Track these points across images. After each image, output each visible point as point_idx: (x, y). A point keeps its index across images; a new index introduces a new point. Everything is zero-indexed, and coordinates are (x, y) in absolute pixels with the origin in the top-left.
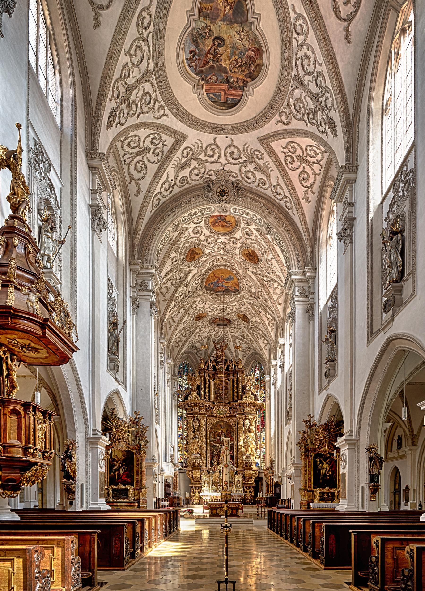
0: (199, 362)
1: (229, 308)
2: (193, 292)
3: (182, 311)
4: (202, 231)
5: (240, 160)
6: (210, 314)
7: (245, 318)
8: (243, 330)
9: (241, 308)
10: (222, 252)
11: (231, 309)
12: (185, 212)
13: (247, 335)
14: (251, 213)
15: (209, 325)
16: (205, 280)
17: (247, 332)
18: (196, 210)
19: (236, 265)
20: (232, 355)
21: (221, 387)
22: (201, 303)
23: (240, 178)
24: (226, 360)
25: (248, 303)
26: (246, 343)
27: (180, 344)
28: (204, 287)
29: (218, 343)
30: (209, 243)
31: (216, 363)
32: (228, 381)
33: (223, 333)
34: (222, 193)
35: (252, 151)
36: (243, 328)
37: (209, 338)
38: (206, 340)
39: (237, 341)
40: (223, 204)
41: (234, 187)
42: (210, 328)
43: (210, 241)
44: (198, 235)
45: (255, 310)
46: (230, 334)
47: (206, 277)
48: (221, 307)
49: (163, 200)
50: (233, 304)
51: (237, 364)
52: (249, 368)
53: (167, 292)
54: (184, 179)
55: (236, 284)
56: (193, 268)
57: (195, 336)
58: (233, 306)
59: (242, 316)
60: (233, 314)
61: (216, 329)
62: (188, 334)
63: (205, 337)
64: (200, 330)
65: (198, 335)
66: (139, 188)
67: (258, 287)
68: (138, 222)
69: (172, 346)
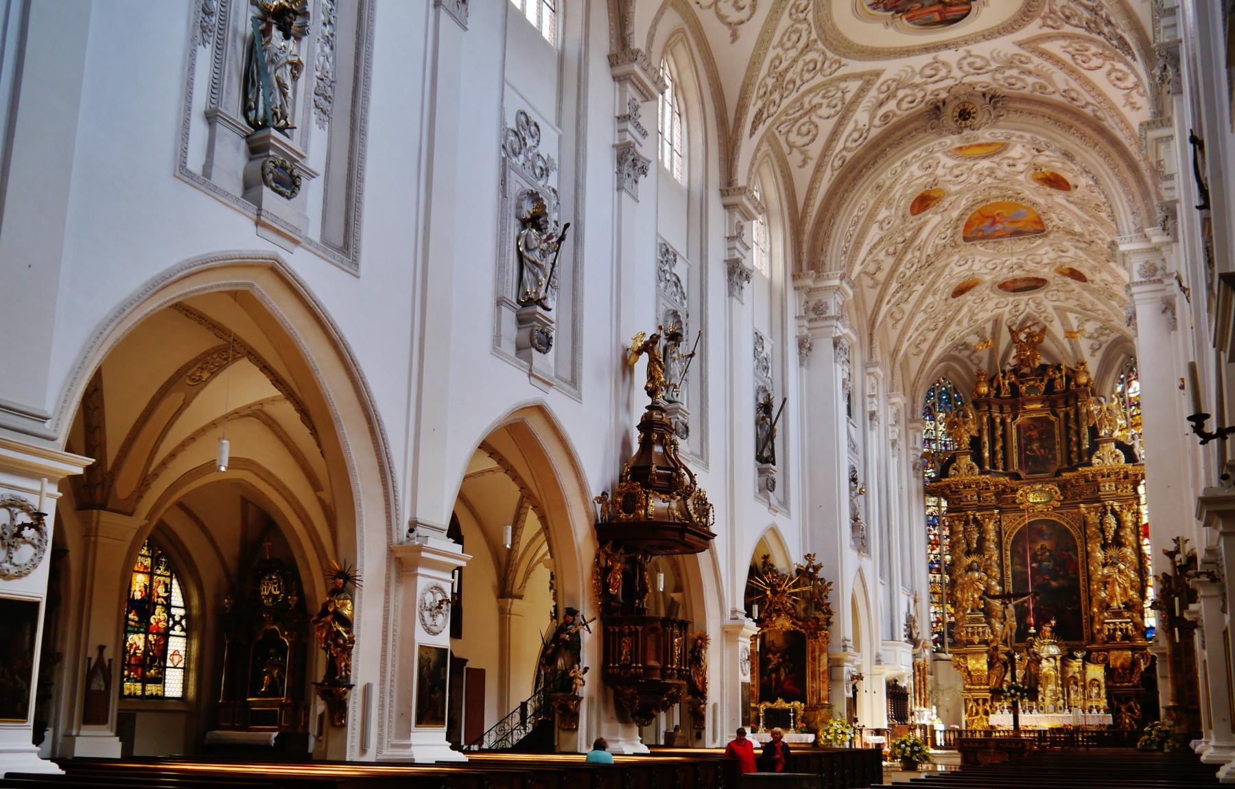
1: (1031, 260)
2: (937, 255)
3: (919, 288)
6: (988, 278)
7: (1076, 275)
8: (1079, 293)
9: (1061, 257)
10: (989, 180)
11: (1038, 259)
12: (894, 162)
13: (1092, 304)
15: (992, 295)
16: (961, 229)
17: (1091, 298)
18: (917, 152)
20: (1063, 350)
21: (1034, 434)
22: (962, 263)
23: (994, 85)
24: (1044, 367)
25: (1076, 247)
26: (1095, 319)
27: (925, 347)
28: (960, 240)
29: (1021, 330)
30: (957, 176)
32: (1052, 418)
33: (1032, 305)
34: (965, 114)
35: (1009, 56)
37: (997, 322)
38: (989, 327)
39: (1071, 317)
40: (967, 132)
42: (996, 301)
43: (959, 173)
44: (929, 171)
45: (1095, 260)
46: (1048, 305)
47: (962, 225)
48: (1014, 260)
49: (849, 156)
50: (1042, 251)
51: (1072, 375)
53: (879, 269)
54: (886, 116)
55: (1035, 222)
56: (930, 216)
57: (959, 323)
58: (1041, 255)
59: (1067, 272)
60: (1046, 270)
61: (1011, 299)
62: (940, 325)
63: (988, 320)
64: (970, 310)
65: (965, 322)
69: (906, 355)
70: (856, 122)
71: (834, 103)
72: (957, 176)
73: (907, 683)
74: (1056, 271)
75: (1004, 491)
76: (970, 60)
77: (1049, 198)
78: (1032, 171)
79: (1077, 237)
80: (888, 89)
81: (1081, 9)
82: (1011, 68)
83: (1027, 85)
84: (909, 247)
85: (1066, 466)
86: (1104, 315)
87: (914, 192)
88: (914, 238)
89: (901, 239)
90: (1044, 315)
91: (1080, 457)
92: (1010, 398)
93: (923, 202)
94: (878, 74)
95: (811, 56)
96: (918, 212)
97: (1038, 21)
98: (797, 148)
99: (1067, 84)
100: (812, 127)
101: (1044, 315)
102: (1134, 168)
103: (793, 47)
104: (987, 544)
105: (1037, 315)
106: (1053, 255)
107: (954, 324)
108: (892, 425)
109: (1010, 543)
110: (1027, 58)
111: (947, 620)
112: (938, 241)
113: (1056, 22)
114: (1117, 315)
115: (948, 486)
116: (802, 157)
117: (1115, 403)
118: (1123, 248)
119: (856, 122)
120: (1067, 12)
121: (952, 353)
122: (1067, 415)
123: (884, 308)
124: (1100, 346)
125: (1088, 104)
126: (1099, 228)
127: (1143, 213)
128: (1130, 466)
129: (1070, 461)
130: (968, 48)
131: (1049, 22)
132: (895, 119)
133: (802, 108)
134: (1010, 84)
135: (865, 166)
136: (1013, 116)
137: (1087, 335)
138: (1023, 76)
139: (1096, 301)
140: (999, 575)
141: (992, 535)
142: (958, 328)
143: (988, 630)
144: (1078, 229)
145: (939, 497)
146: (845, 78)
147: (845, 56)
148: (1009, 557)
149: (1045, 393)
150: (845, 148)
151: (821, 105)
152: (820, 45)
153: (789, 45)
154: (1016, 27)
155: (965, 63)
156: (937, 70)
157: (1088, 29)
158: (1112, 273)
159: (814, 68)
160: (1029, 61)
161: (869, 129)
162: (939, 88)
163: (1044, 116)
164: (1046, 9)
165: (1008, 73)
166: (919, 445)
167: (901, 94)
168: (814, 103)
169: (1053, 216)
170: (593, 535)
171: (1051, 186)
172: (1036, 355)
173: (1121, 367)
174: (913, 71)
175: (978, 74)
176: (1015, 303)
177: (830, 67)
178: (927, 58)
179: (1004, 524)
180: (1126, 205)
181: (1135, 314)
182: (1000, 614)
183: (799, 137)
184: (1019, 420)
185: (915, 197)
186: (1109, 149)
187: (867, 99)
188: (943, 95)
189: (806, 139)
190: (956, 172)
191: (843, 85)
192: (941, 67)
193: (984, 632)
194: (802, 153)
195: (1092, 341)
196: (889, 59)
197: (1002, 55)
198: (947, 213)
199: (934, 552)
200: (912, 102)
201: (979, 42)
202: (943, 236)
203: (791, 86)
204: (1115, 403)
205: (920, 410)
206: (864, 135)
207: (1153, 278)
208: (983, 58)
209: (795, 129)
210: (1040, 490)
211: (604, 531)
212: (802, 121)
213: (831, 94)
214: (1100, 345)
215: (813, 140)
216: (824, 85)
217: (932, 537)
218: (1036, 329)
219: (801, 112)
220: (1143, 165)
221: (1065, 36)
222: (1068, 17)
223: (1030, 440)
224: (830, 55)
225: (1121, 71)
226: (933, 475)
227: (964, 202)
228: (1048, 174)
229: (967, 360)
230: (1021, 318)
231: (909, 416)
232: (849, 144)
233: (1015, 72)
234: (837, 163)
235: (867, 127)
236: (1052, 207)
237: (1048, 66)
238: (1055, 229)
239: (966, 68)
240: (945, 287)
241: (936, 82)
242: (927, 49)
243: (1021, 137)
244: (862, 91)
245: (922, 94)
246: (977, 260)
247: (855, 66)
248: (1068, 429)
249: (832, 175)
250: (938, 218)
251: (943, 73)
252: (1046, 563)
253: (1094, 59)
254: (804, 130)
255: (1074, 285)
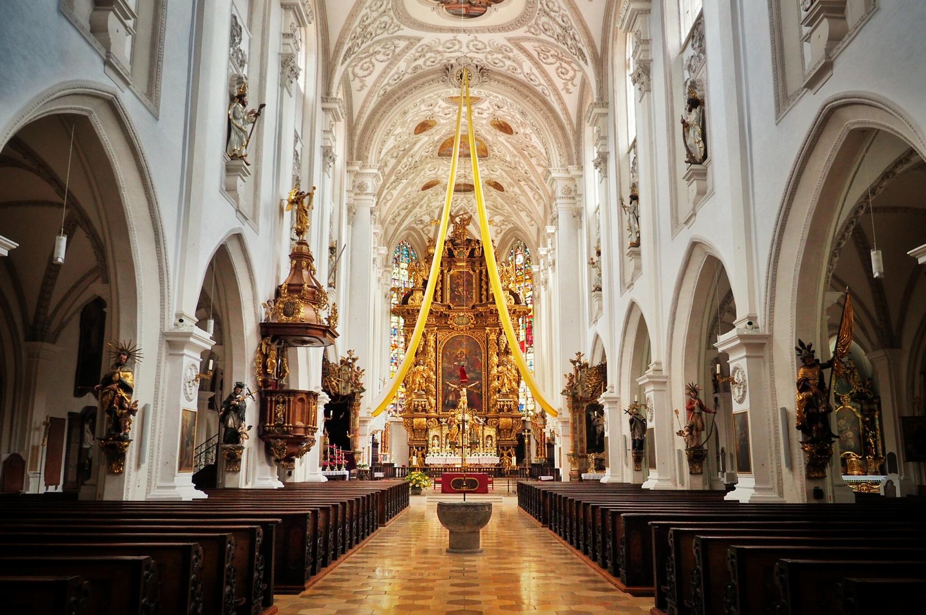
0: (428, 244)
2: (421, 162)
4: (437, 104)
5: (485, 50)
7: (498, 187)
12: (416, 99)
13: (502, 205)
14: (500, 97)
16: (439, 147)
17: (502, 201)
18: (431, 95)
19: (483, 131)
21: (461, 281)
22: (432, 169)
23: (485, 62)
24: (469, 241)
25: (502, 170)
26: (501, 215)
27: (398, 219)
30: (446, 114)
31: (453, 245)
32: (471, 272)
35: (499, 45)
36: (495, 195)
38: (437, 211)
41: (478, 71)
43: (448, 112)
44: (431, 108)
45: (512, 179)
47: (440, 144)
49: (389, 89)
52: (506, 250)
54: (416, 68)
55: (483, 151)
57: (421, 207)
62: (410, 206)
65: (425, 206)
66: (364, 84)
67: (515, 156)
68: (359, 117)
70: (398, 68)
71: (388, 52)
72: (446, 114)
73: (378, 437)
74: (486, 182)
75: (441, 316)
76: (475, 43)
77: (495, 137)
78: (492, 119)
79: (507, 164)
80: (422, 51)
81: (557, 27)
82: (499, 53)
83: (505, 65)
84: (406, 154)
85: (478, 303)
86: (507, 213)
87: (419, 119)
88: (410, 149)
89: (403, 149)
90: (471, 208)
91: (487, 299)
92: (448, 258)
93: (423, 127)
94: (419, 40)
95: (385, 18)
96: (419, 133)
97: (525, 28)
98: (358, 77)
99: (531, 70)
100: (371, 65)
101: (471, 208)
102: (562, 128)
103: (377, 10)
104: (429, 348)
105: (466, 208)
106: (486, 172)
107: (418, 206)
108: (379, 268)
109: (442, 349)
110: (510, 49)
111: (400, 396)
112: (423, 153)
113: (536, 31)
114: (515, 214)
115: (408, 310)
116: (360, 84)
117: (511, 267)
118: (554, 175)
119: (398, 68)
120: (546, 27)
121: (413, 225)
122: (481, 272)
123: (385, 191)
124: (501, 231)
125: (540, 84)
126: (522, 160)
127: (565, 155)
128: (517, 307)
129: (481, 301)
130: (477, 35)
131: (532, 30)
132: (419, 71)
133: (368, 52)
134: (494, 63)
135: (398, 98)
136: (494, 84)
137: (494, 224)
138: (504, 60)
139: (505, 204)
140: (434, 369)
141: (432, 343)
142: (420, 210)
143: (427, 404)
144: (508, 159)
145: (399, 316)
146: (399, 38)
147: (404, 25)
148: (441, 358)
149: (468, 257)
150: (388, 84)
151: (380, 52)
152: (392, 13)
153: (374, 8)
154: (511, 28)
155: (471, 44)
156: (454, 45)
157: (558, 39)
158: (520, 188)
159: (385, 27)
160: (511, 51)
161: (404, 74)
162: (450, 57)
163: (512, 87)
164: (533, 22)
165: (495, 56)
166: (389, 282)
167: (428, 55)
168: (375, 50)
169: (495, 149)
170: (257, 331)
171: (501, 130)
172: (464, 232)
173: (512, 245)
174: (439, 43)
175: (477, 53)
176: (455, 199)
177: (393, 29)
178: (450, 36)
179: (438, 336)
180: (556, 149)
181: (558, 216)
182: (434, 393)
183: (361, 71)
184: (452, 272)
185: (419, 123)
186: (550, 115)
187: (408, 54)
188: (453, 61)
189: (366, 73)
190: (446, 111)
191: (397, 42)
192: (456, 42)
193: (425, 405)
194: (362, 81)
195: (497, 228)
196: (428, 31)
197: (495, 44)
198: (432, 136)
199: (394, 352)
200: (433, 62)
201: (485, 33)
202: (427, 150)
203: (369, 36)
204: (511, 267)
205: (391, 259)
206: (401, 77)
207: (569, 196)
208: (483, 43)
209: (360, 65)
210: (463, 316)
211: (267, 330)
212: (365, 60)
213: (388, 46)
214: (501, 231)
215: (370, 74)
216: (387, 39)
217: (393, 342)
218: (466, 216)
219: (367, 54)
220: (568, 128)
221: (539, 41)
222: (546, 30)
223: (458, 285)
224: (395, 20)
225: (565, 68)
226: (397, 302)
227: (444, 131)
228: (501, 123)
229: (421, 231)
230: (457, 208)
231: (385, 264)
232: (390, 82)
233: (500, 56)
234: (382, 92)
235: (403, 73)
236: (496, 143)
237: (522, 57)
238: (494, 157)
239: (471, 47)
240: (420, 183)
241: (451, 52)
242: (452, 30)
243: (496, 97)
244: (407, 48)
245: (441, 58)
246: (440, 170)
247: (407, 31)
248: (481, 280)
249: (377, 100)
250: (426, 139)
251: (456, 47)
252: (463, 363)
253: (551, 58)
254: (365, 66)
255: (494, 192)
